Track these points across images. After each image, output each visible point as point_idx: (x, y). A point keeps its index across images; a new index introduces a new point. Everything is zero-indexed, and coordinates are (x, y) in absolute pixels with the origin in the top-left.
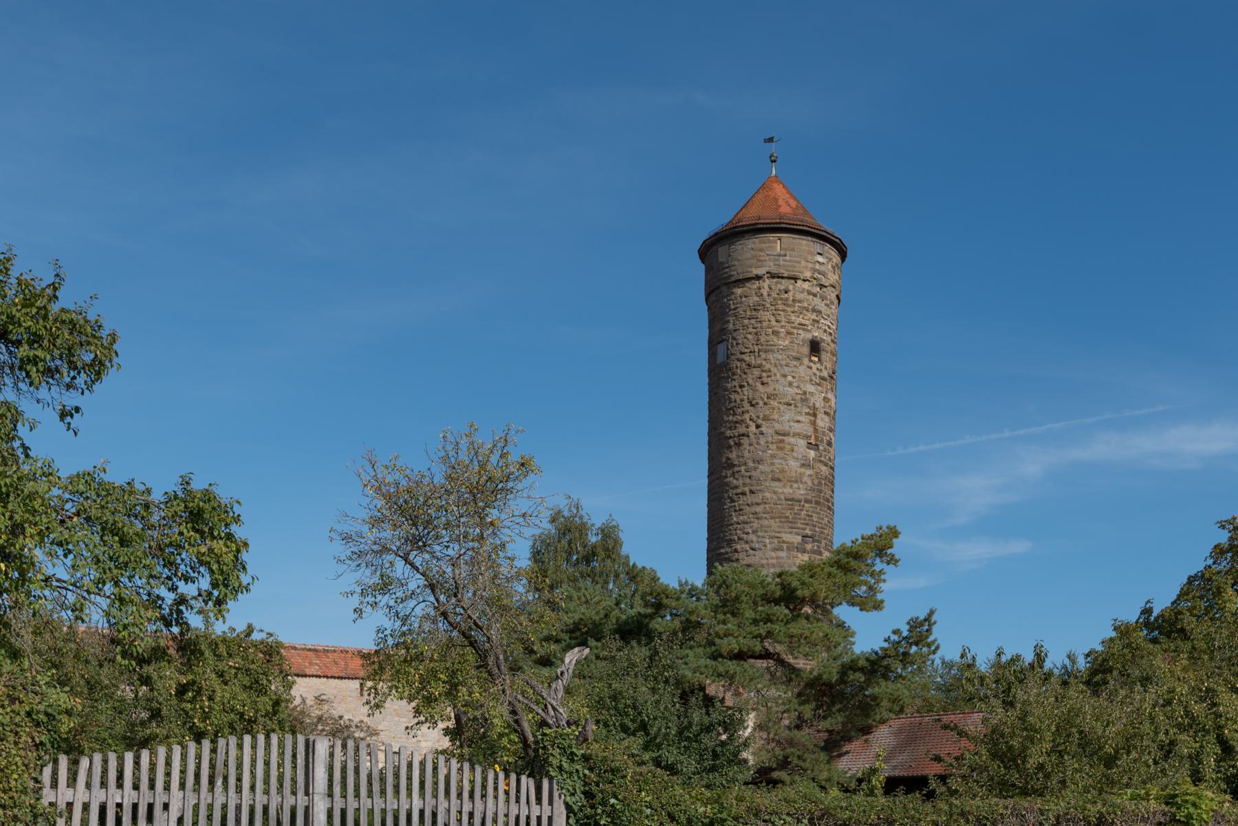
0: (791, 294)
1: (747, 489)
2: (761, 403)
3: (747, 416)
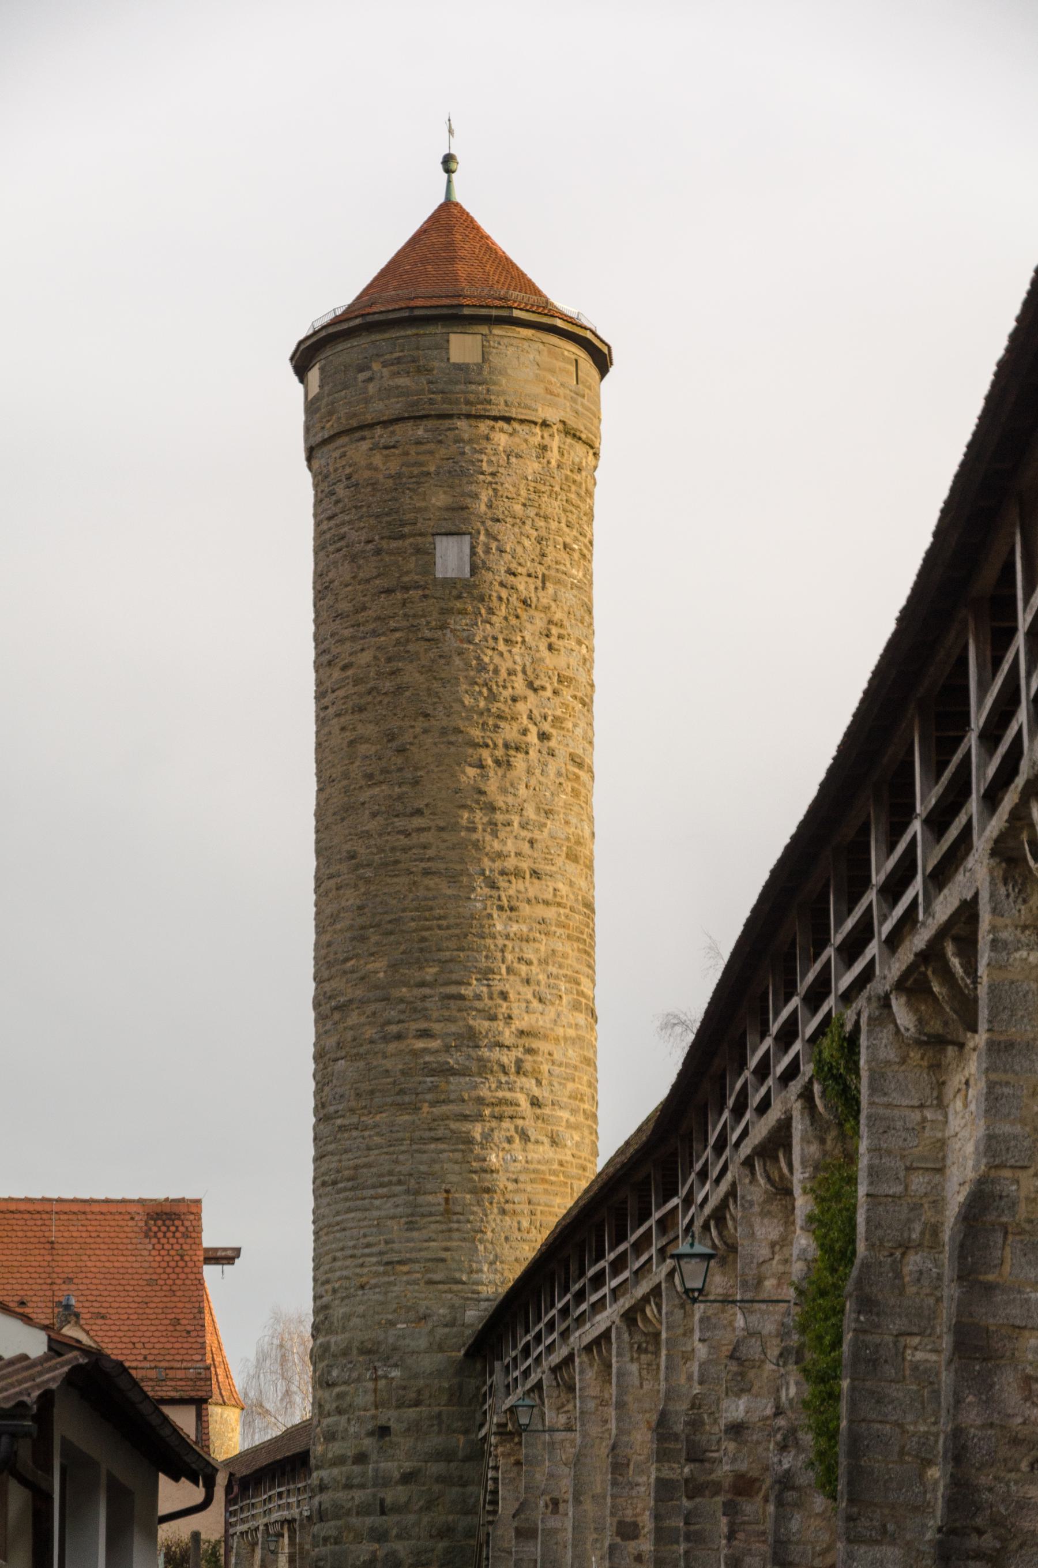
0: (584, 473)
1: (525, 865)
2: (549, 693)
3: (521, 707)
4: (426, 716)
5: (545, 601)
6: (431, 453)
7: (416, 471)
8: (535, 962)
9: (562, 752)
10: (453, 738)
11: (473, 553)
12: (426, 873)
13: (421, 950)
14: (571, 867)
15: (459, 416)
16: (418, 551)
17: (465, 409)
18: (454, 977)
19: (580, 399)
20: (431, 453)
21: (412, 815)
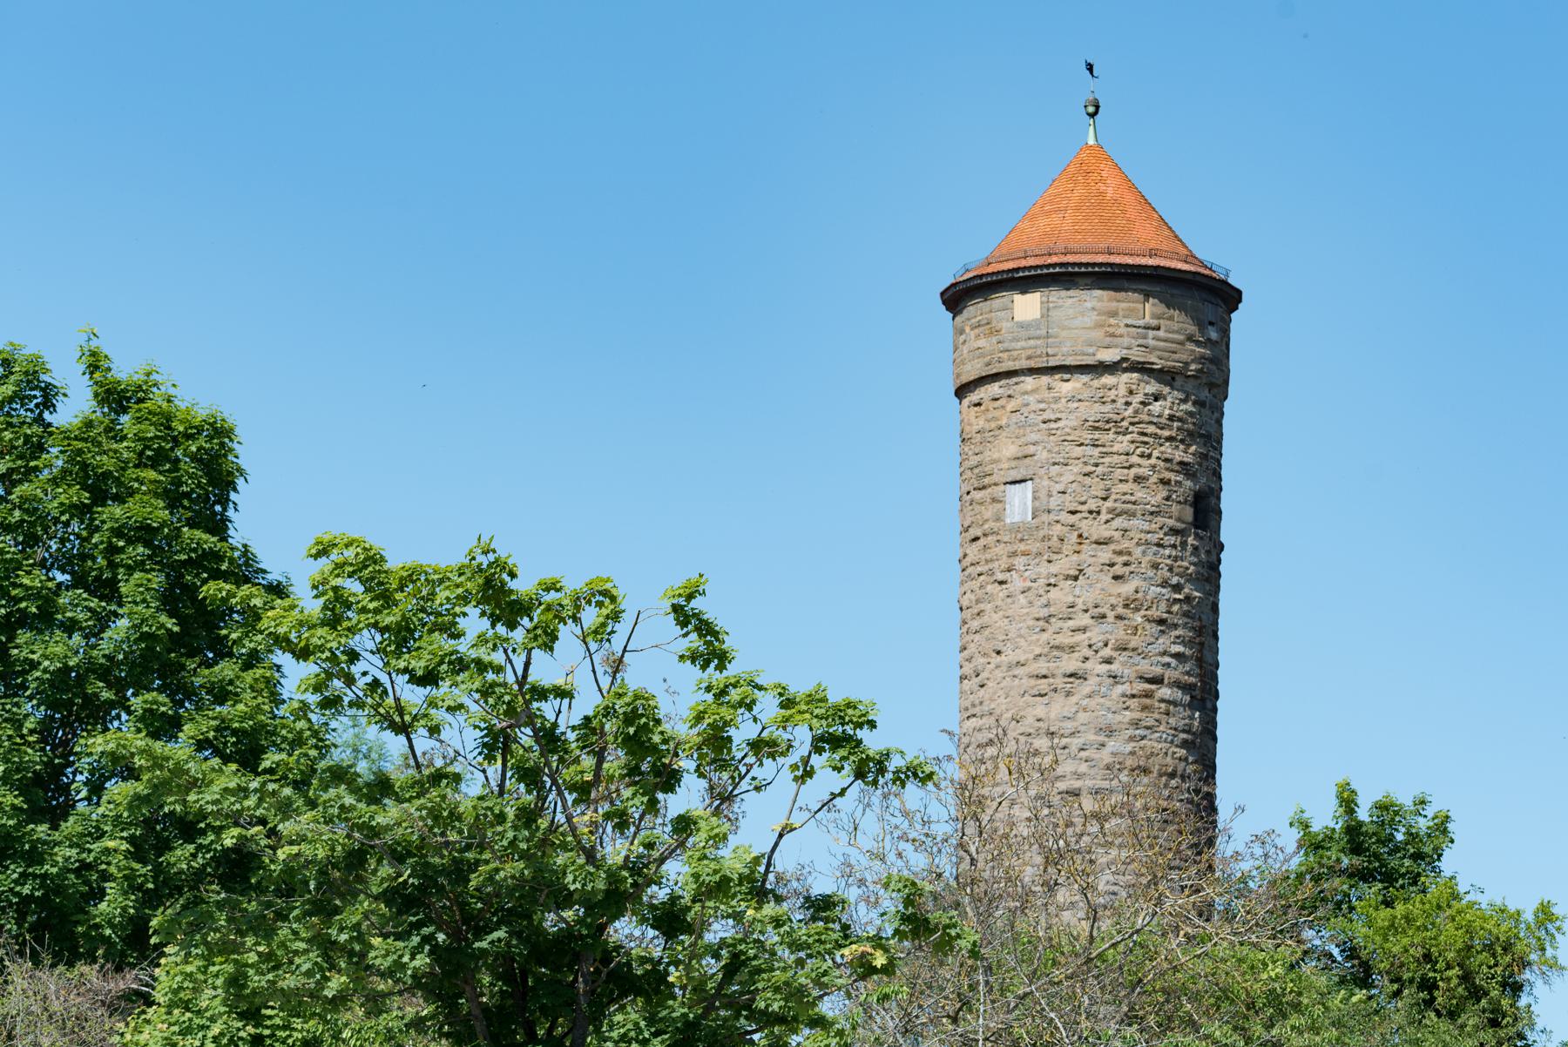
2: (1111, 618)
3: (1079, 637)
4: (999, 653)
5: (1107, 534)
7: (993, 425)
10: (1016, 672)
11: (1035, 498)
16: (994, 500)
19: (1151, 333)
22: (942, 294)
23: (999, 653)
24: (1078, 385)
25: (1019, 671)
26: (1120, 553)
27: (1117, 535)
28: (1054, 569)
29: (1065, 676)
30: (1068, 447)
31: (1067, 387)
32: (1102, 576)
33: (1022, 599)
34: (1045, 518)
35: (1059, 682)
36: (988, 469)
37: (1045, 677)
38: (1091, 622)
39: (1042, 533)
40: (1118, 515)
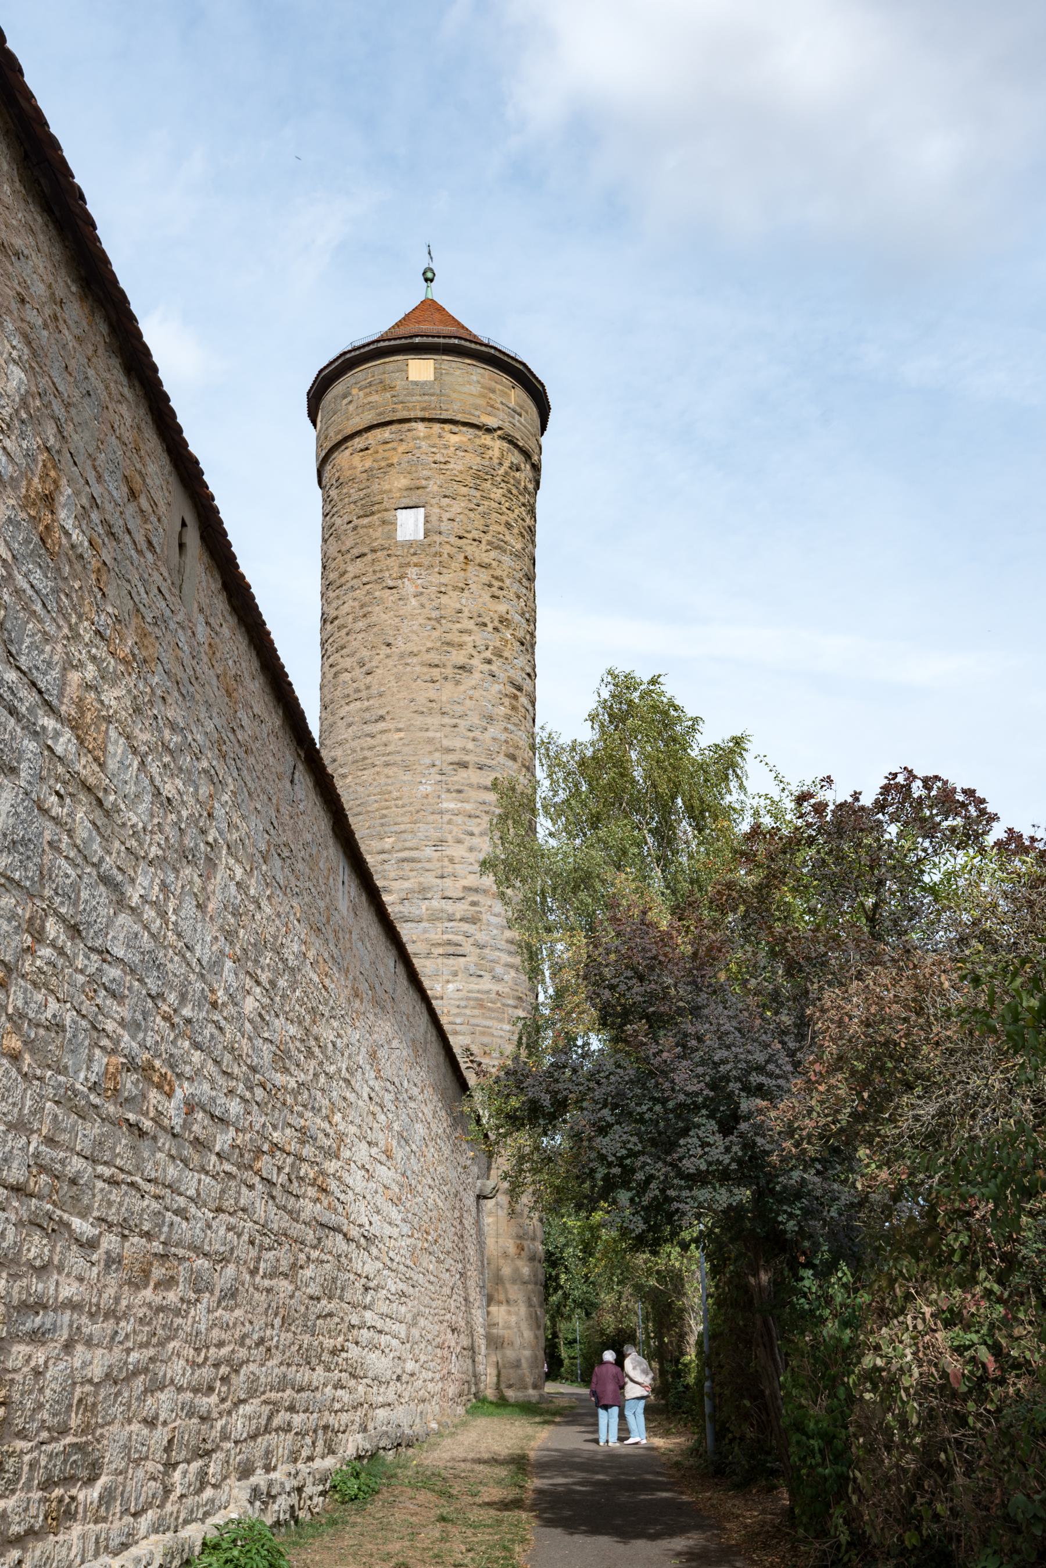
2: (490, 626)
3: (466, 638)
4: (389, 645)
5: (487, 561)
6: (394, 449)
8: (476, 831)
9: (502, 676)
11: (426, 522)
12: (387, 765)
13: (382, 825)
14: (510, 763)
15: (416, 420)
16: (384, 522)
17: (420, 414)
18: (408, 844)
20: (394, 449)
21: (376, 721)
22: (321, 372)
23: (389, 645)
24: (465, 439)
25: (414, 660)
26: (497, 578)
27: (495, 564)
28: (443, 579)
29: (455, 667)
30: (456, 486)
31: (454, 439)
32: (483, 593)
33: (414, 602)
34: (437, 538)
35: (449, 671)
36: (378, 498)
37: (437, 666)
38: (475, 628)
39: (433, 550)
40: (496, 548)
